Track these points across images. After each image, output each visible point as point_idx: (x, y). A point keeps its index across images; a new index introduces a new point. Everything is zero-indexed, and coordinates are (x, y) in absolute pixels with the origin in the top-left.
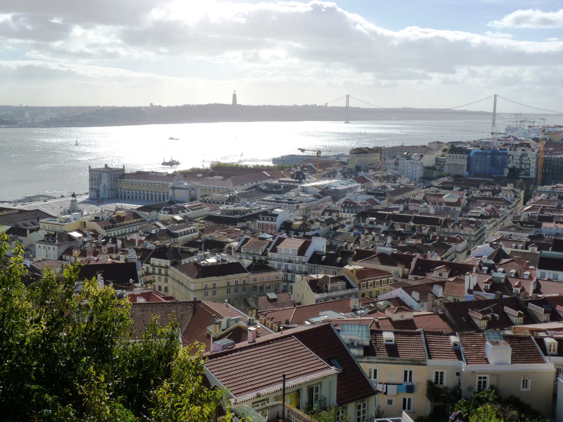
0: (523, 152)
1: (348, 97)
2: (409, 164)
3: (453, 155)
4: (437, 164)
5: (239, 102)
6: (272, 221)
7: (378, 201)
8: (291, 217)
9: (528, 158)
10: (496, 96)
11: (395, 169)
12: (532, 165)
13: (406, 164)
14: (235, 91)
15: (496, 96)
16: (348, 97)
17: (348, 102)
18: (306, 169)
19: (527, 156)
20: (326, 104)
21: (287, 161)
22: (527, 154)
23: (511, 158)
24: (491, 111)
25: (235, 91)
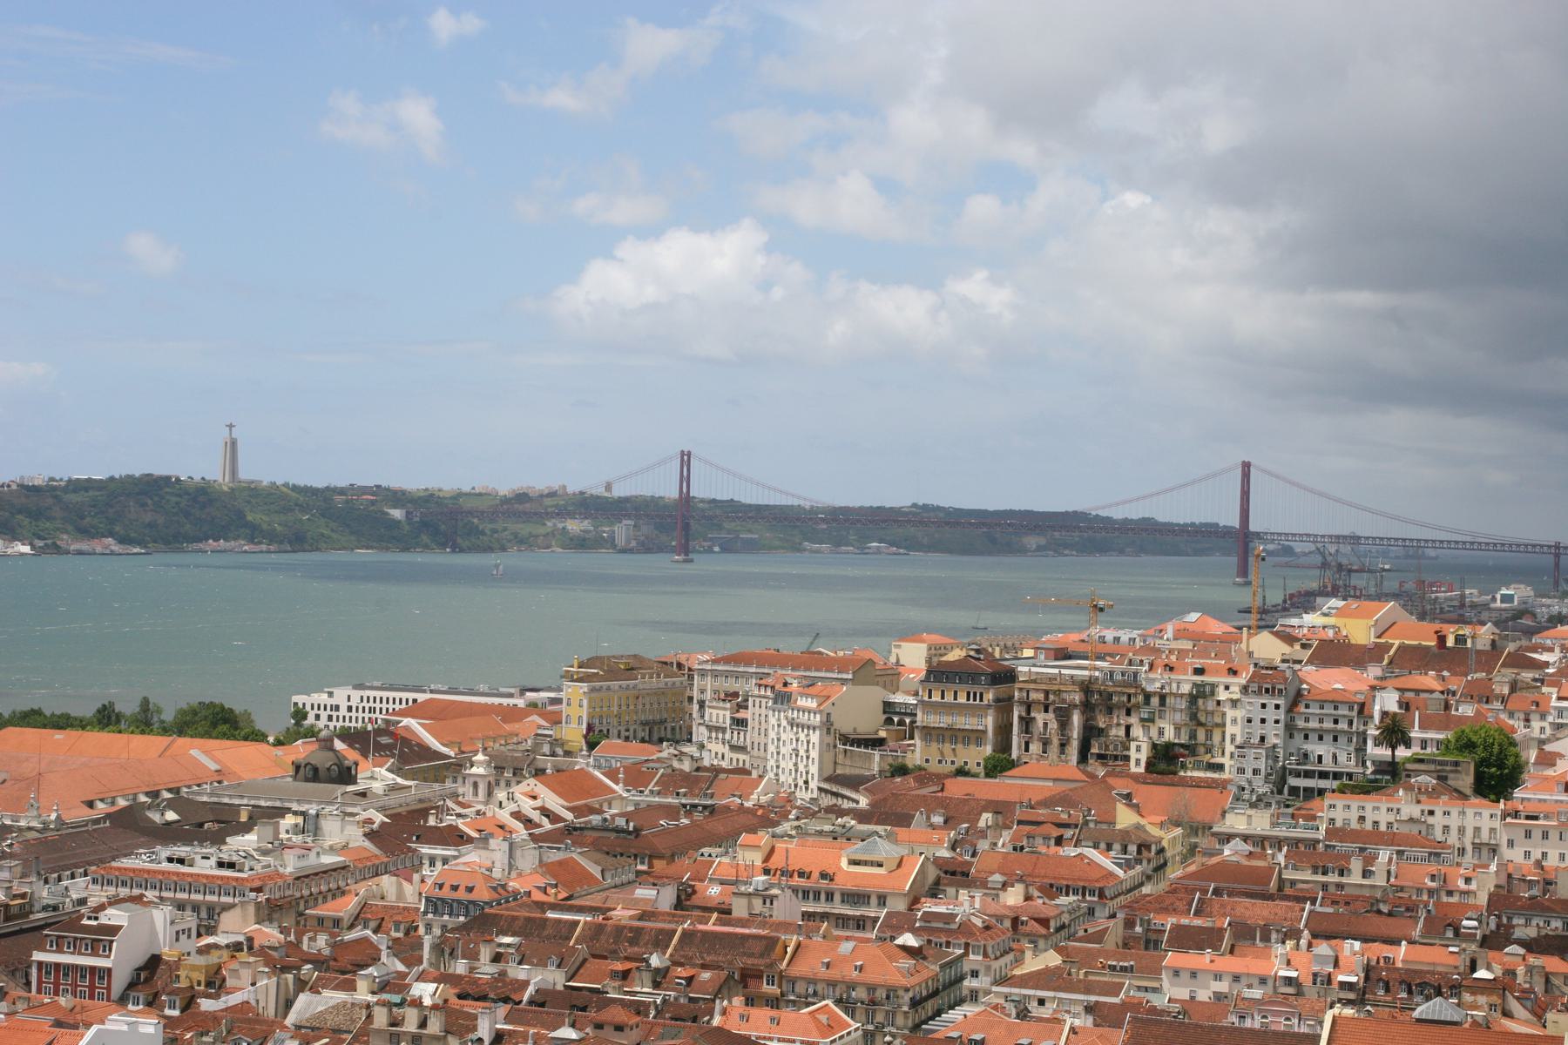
0: (1198, 679)
1: (686, 458)
2: (784, 723)
3: (942, 686)
4: (889, 721)
5: (245, 474)
6: (95, 954)
7: (595, 871)
8: (183, 937)
9: (1219, 703)
10: (1246, 466)
11: (734, 748)
12: (1230, 730)
13: (773, 721)
14: (231, 426)
15: (1246, 466)
16: (686, 458)
17: (685, 479)
18: (385, 740)
19: (1213, 693)
20: (608, 487)
21: (350, 709)
22: (1213, 686)
23: (1155, 701)
24: (1234, 521)
25: (231, 426)
